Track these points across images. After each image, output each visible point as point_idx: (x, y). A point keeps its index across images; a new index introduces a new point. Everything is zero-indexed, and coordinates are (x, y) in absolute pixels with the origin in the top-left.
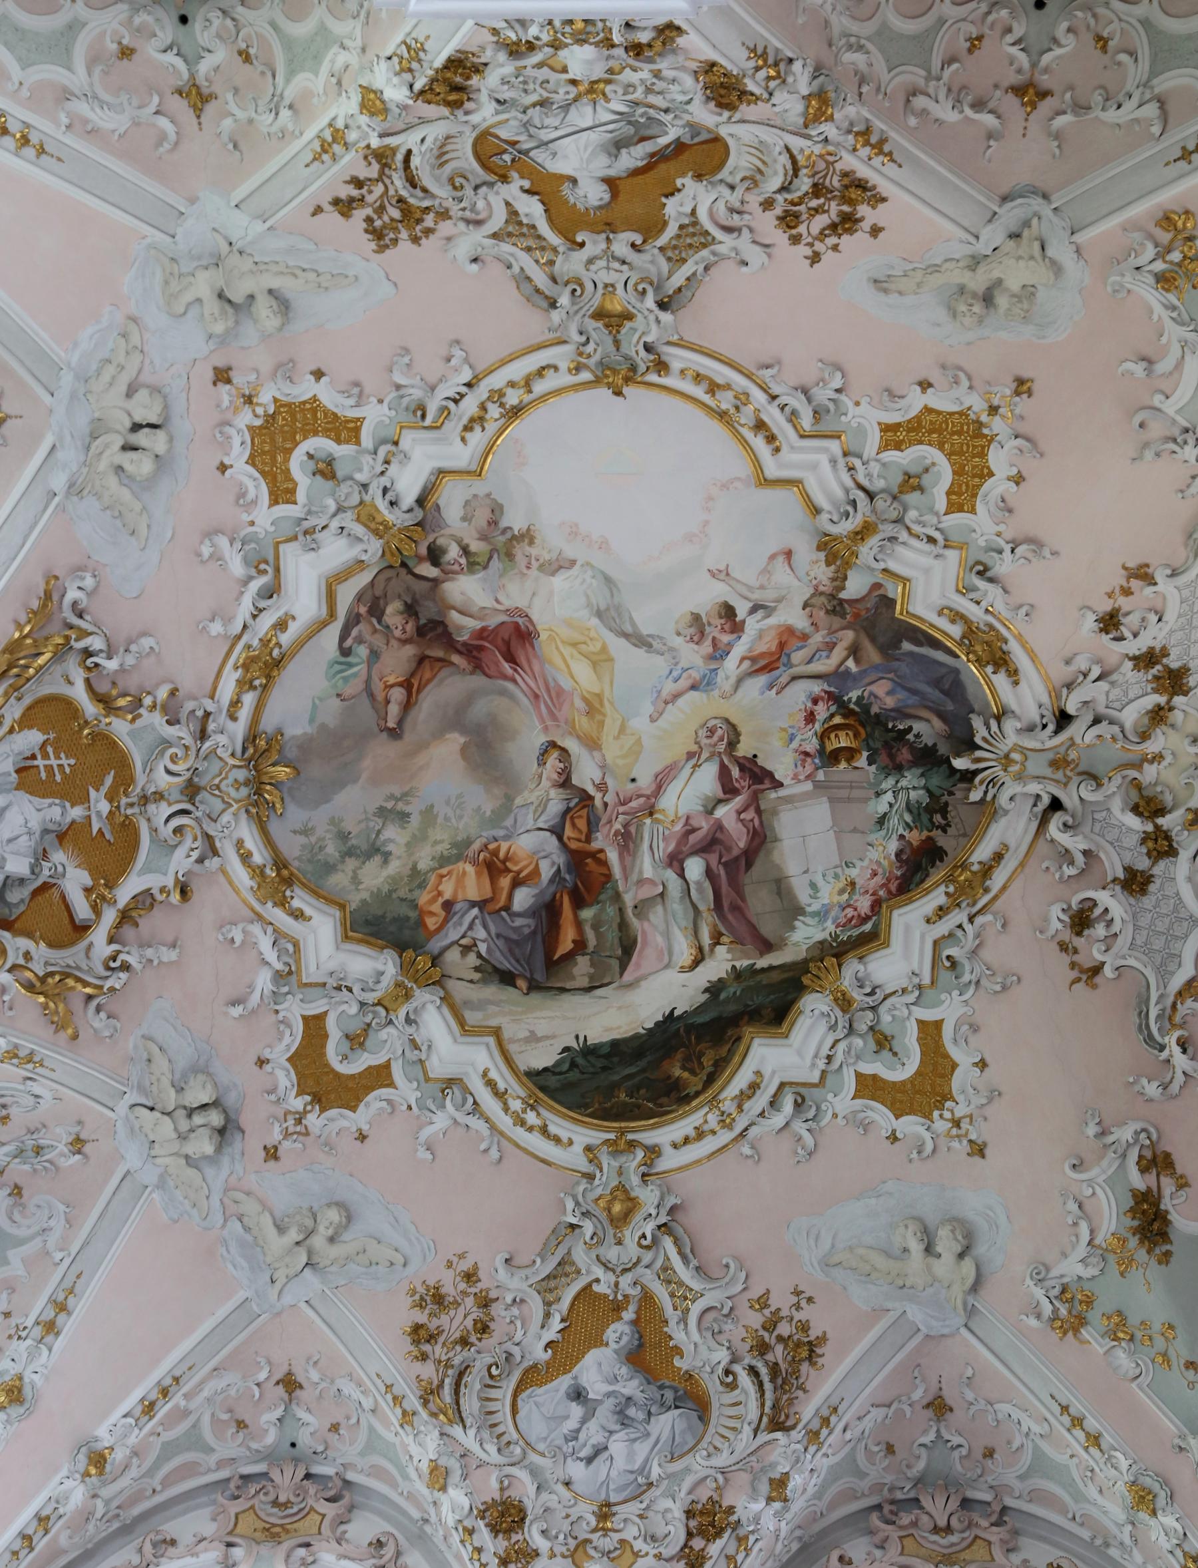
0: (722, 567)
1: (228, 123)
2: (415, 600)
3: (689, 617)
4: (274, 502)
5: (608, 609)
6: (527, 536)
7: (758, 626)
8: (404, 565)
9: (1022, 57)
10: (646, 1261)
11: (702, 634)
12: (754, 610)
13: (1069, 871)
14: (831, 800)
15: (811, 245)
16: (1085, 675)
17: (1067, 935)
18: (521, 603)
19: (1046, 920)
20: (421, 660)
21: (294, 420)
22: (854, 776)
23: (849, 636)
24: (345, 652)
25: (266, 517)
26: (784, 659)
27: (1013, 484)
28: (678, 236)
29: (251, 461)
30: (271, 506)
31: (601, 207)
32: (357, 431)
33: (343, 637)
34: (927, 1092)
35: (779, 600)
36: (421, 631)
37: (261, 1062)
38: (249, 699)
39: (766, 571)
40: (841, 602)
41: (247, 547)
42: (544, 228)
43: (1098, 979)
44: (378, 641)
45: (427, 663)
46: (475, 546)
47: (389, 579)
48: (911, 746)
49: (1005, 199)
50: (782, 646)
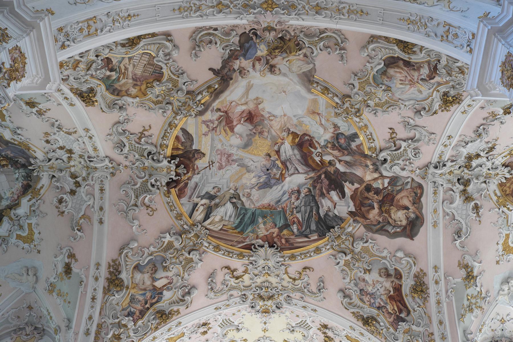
13: (58, 191)
14: (5, 175)
17: (57, 204)
19: (53, 201)
22: (8, 170)
34: (29, 239)
43: (64, 214)
48: (20, 164)
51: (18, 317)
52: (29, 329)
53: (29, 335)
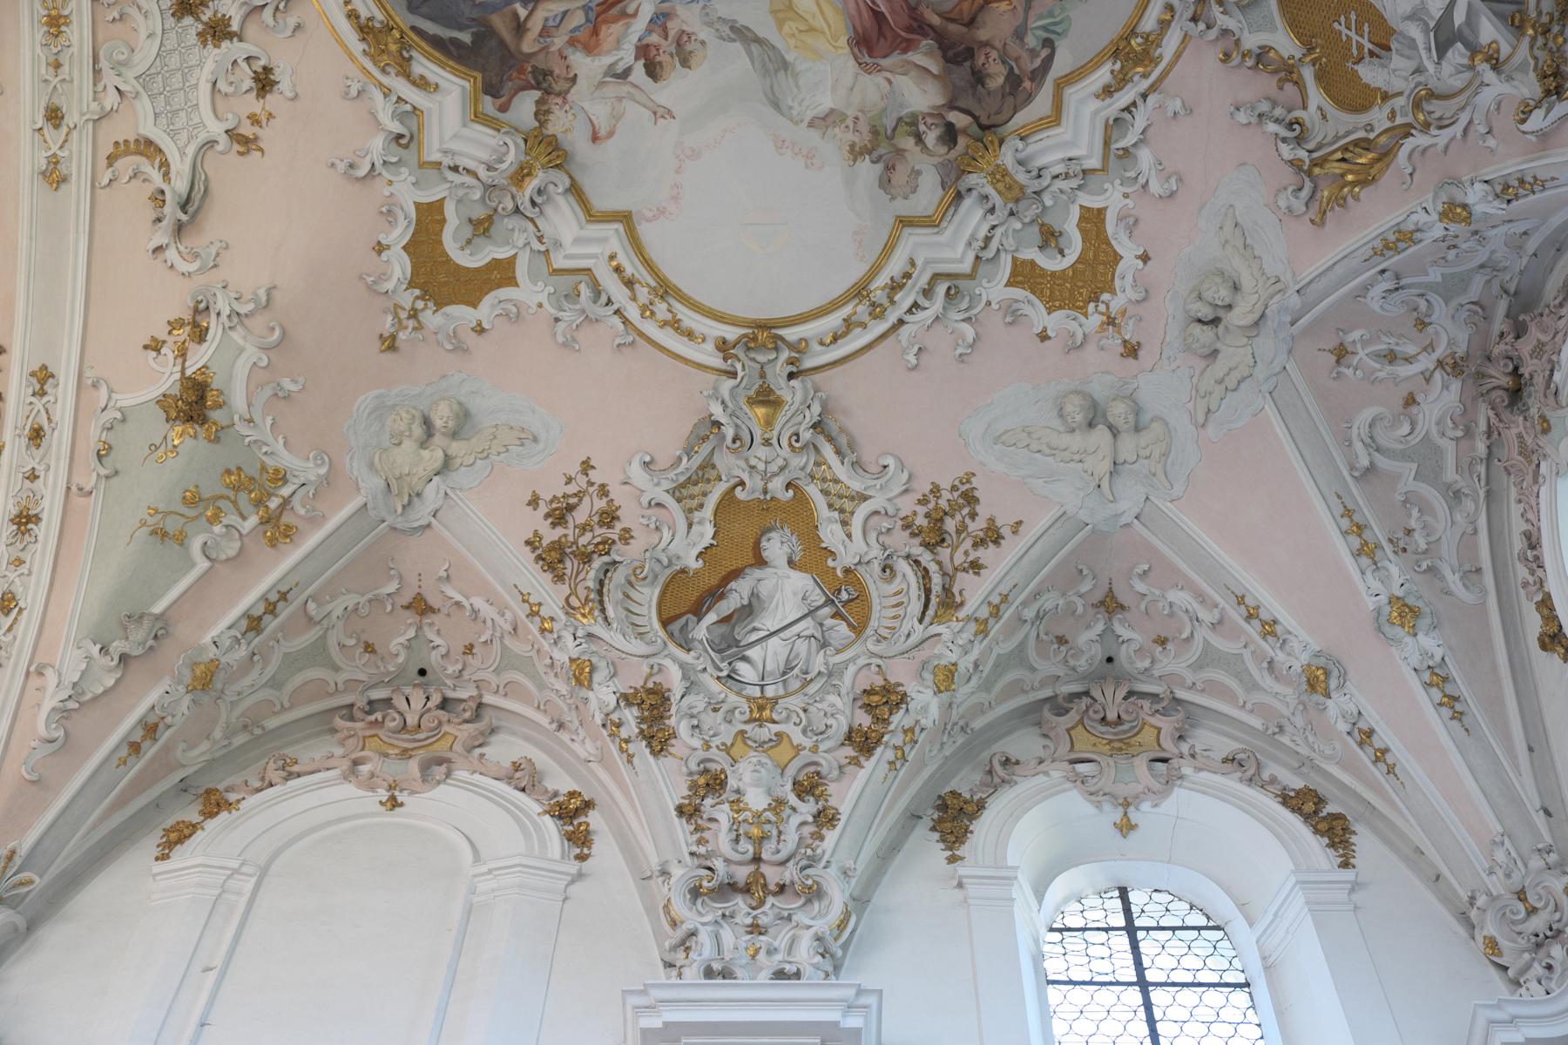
0: (661, 121)
1: (1085, 587)
2: (974, 87)
3: (693, 62)
4: (1101, 212)
5: (776, 71)
6: (856, 153)
7: (621, 54)
8: (983, 128)
9: (431, 635)
11: (679, 44)
12: (626, 73)
15: (591, 484)
16: (277, 8)
18: (866, 79)
20: (971, 23)
21: (1071, 291)
23: (528, 46)
24: (1048, 43)
25: (1111, 198)
26: (592, 15)
27: (384, 242)
28: (705, 494)
29: (1117, 258)
30: (1105, 209)
31: (770, 530)
32: (1014, 273)
33: (1049, 60)
35: (602, 84)
36: (970, 53)
38: (1149, 24)
39: (616, 117)
40: (538, 87)
41: (1132, 174)
42: (819, 501)
44: (1014, 49)
45: (966, 20)
46: (909, 143)
47: (998, 113)
49: (429, 526)
50: (595, 32)
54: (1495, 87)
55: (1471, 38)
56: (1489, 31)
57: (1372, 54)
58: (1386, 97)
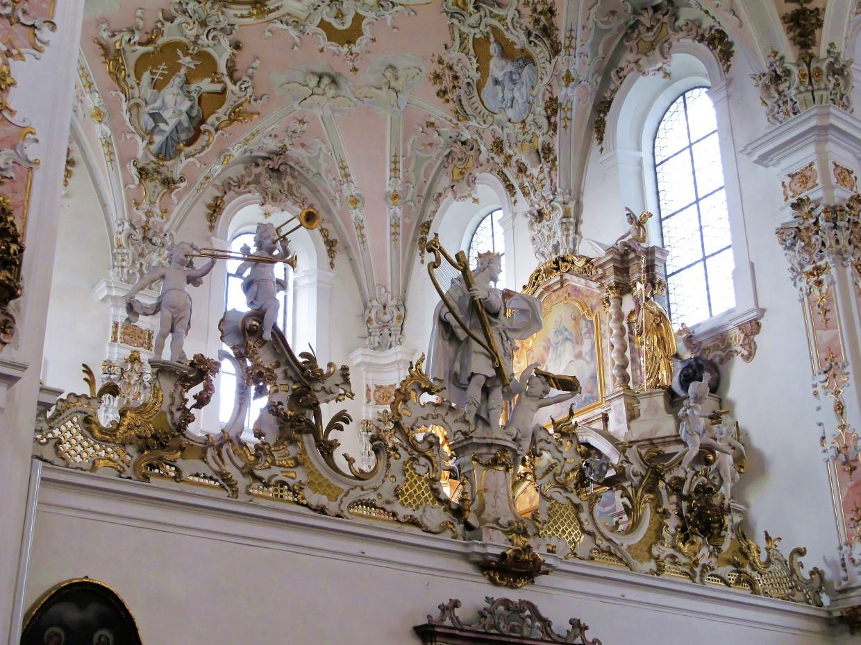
10: (483, 15)
37: (322, 50)
51: (613, 13)
52: (646, 19)
53: (652, 27)
54: (141, 145)
55: (156, 131)
56: (158, 139)
57: (153, 79)
58: (138, 84)
